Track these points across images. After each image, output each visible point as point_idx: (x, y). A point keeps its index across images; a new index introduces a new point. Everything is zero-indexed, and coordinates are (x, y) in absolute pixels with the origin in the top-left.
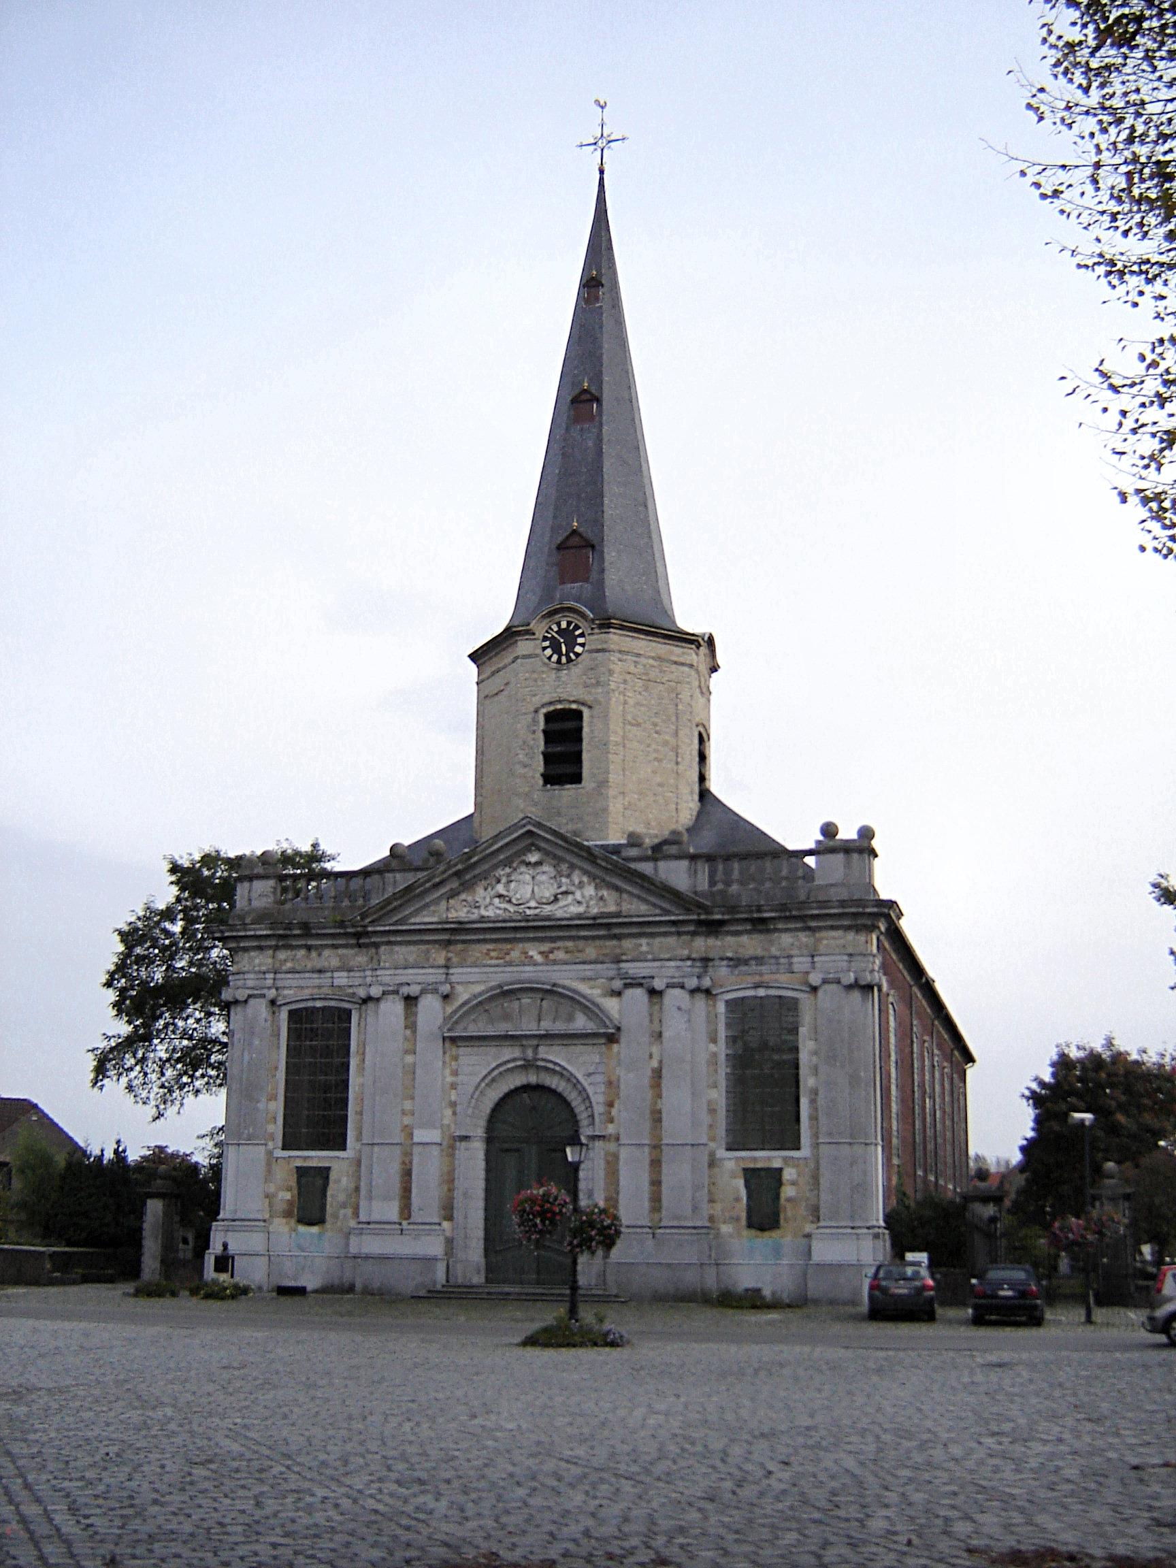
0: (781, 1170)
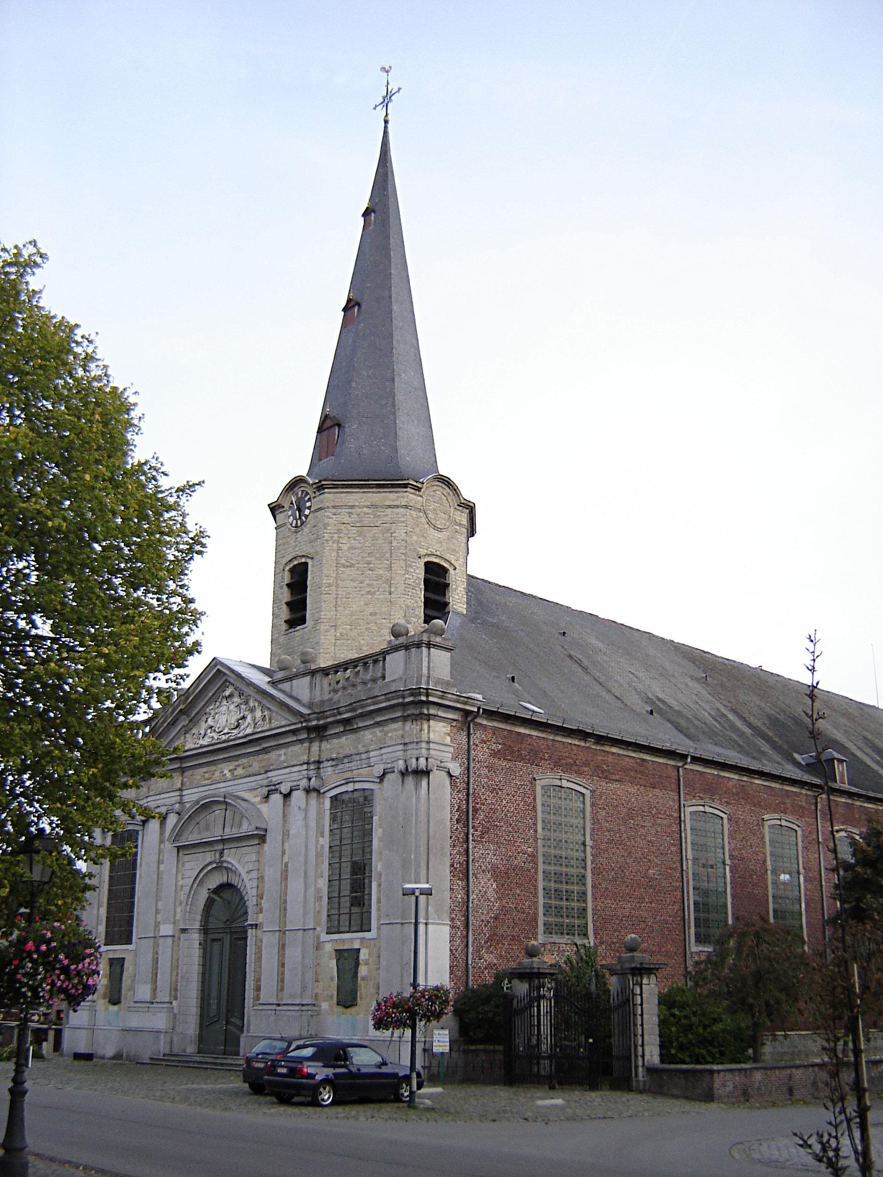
0: (359, 949)
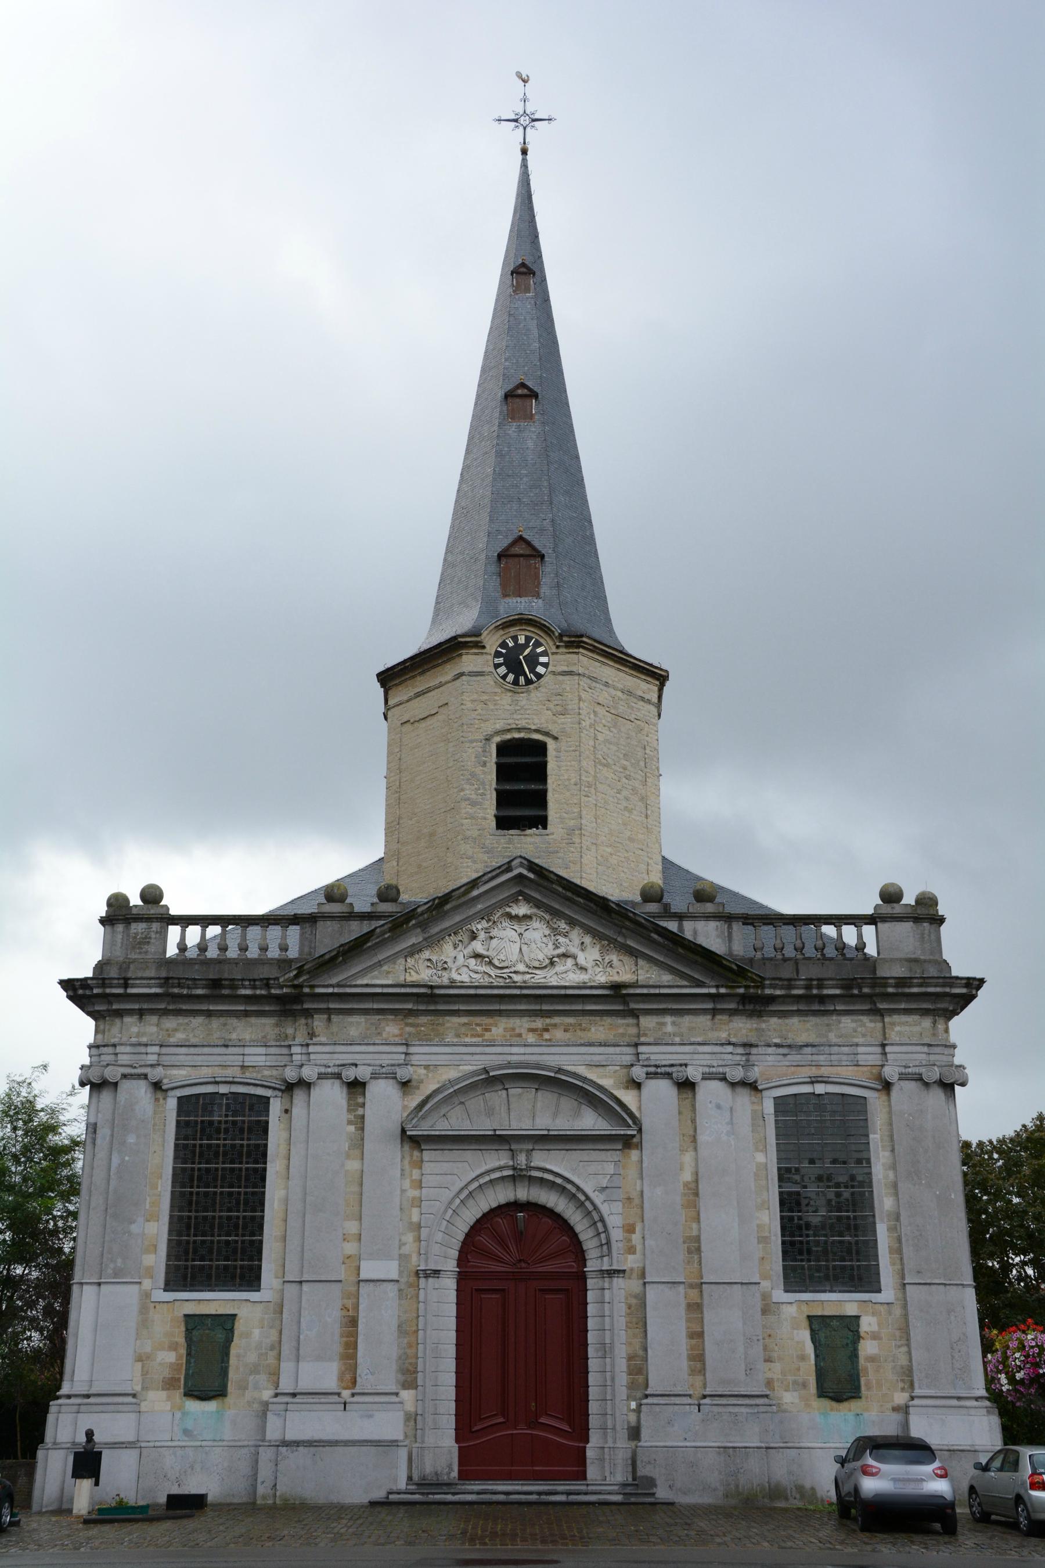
0: (858, 1317)
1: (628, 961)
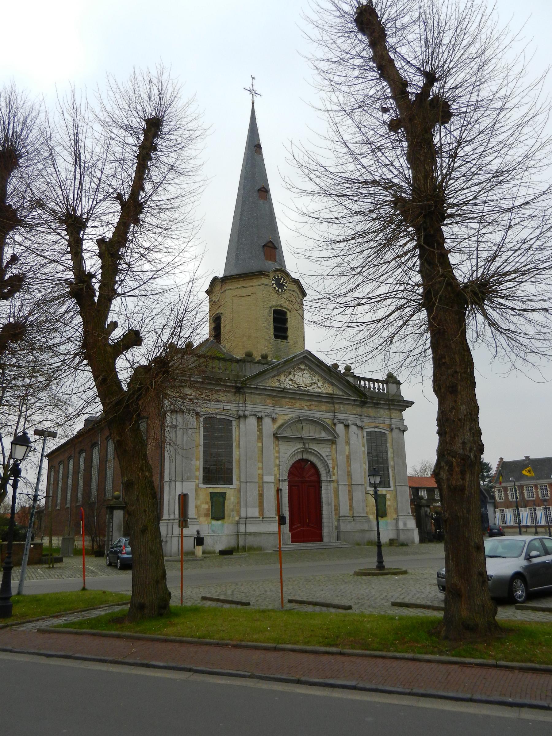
1: (331, 387)
